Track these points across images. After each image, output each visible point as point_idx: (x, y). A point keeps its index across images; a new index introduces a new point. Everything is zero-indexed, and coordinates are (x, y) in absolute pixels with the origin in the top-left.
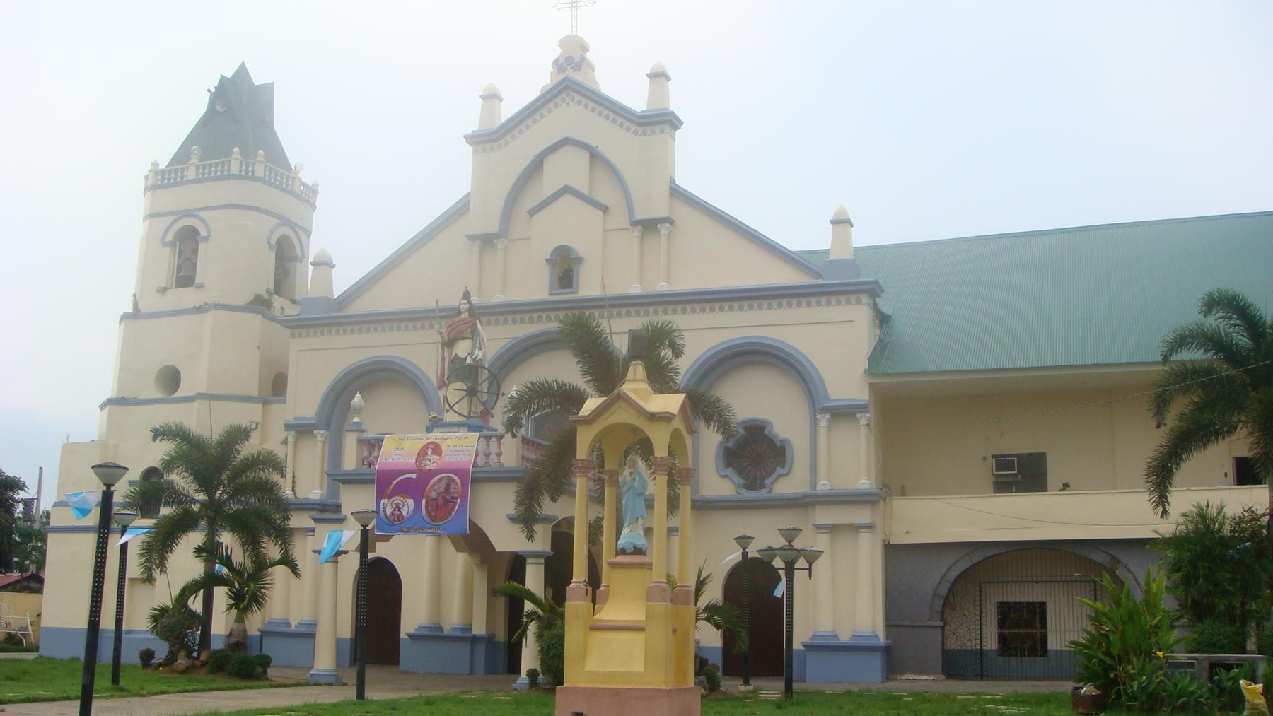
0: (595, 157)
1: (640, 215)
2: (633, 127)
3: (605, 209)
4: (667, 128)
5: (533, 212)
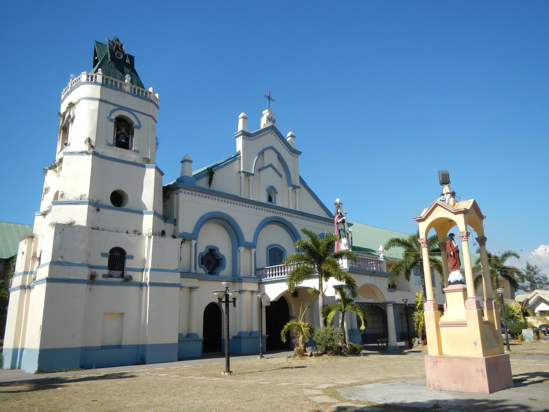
0: (280, 158)
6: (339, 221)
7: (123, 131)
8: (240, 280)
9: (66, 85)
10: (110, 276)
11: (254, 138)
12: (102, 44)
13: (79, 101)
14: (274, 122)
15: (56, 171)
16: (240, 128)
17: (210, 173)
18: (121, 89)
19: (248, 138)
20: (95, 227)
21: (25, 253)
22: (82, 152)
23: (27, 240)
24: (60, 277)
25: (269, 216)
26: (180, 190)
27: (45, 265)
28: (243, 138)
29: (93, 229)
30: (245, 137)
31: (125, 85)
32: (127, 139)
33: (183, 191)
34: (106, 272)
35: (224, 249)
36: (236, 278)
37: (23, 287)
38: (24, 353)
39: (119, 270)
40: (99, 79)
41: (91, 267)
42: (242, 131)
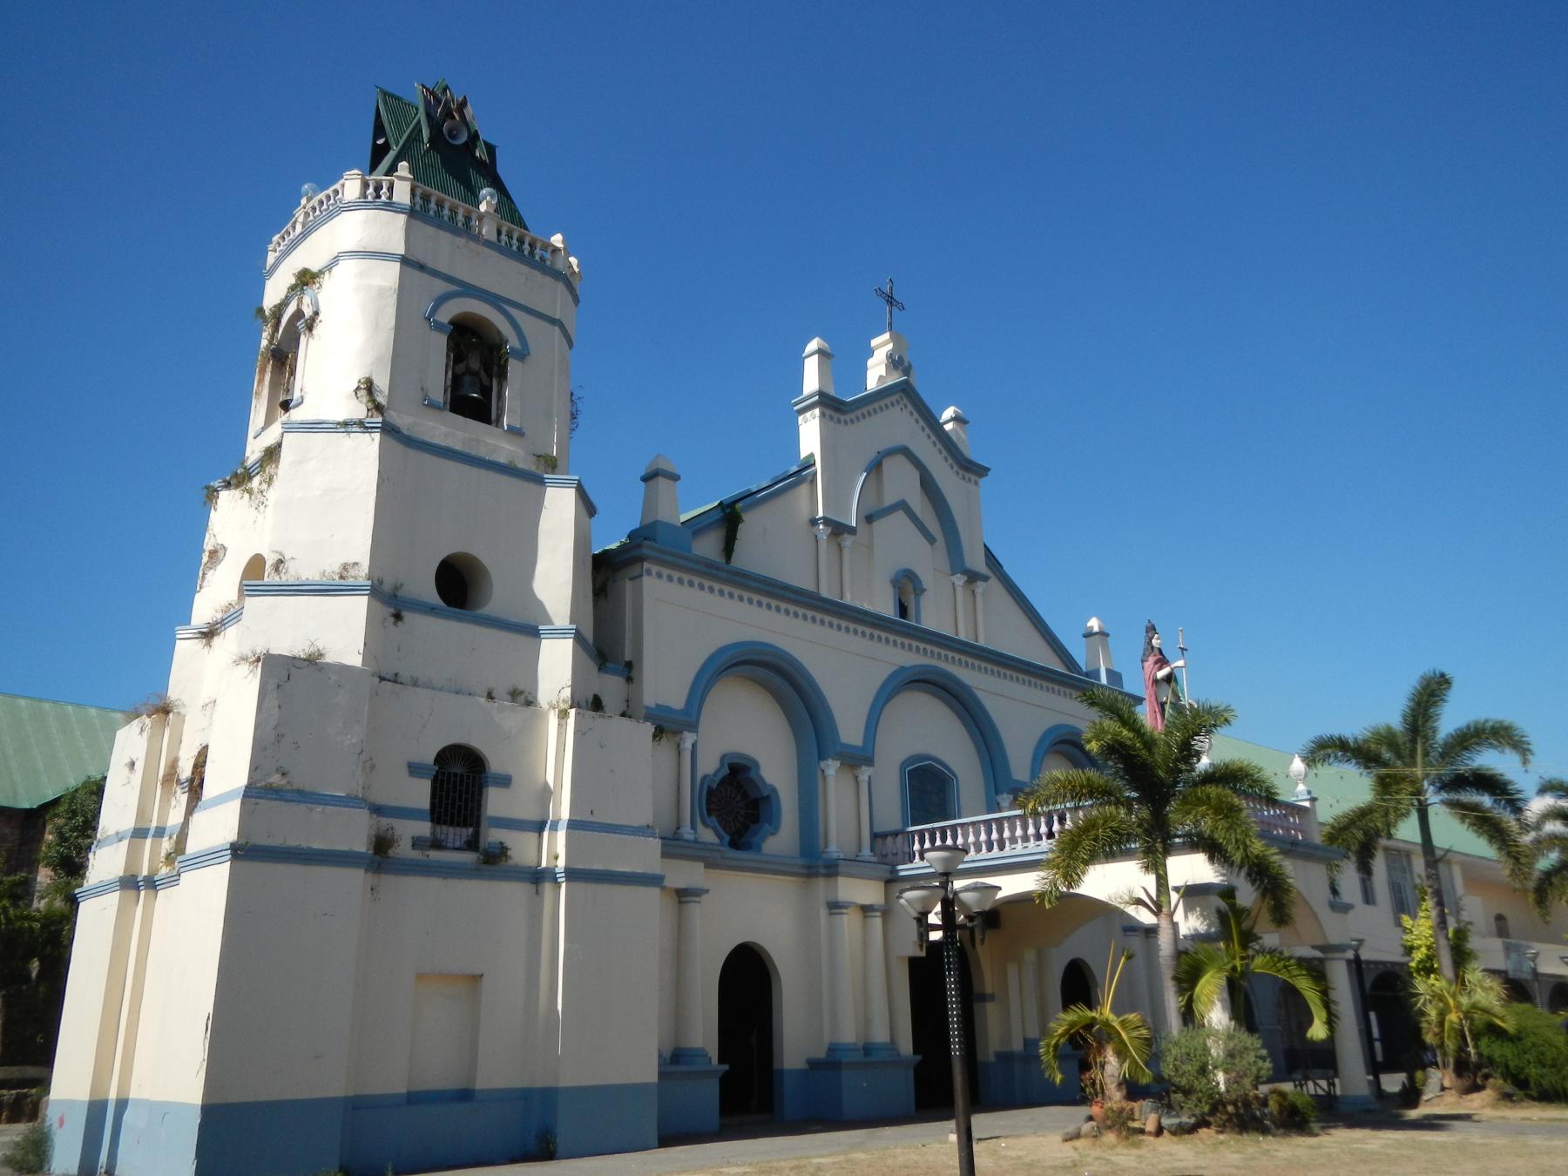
0: (928, 484)
6: (1161, 674)
7: (474, 363)
8: (831, 870)
9: (289, 215)
10: (437, 844)
11: (853, 416)
12: (398, 99)
13: (335, 261)
14: (907, 371)
15: (250, 492)
16: (811, 380)
17: (729, 517)
18: (466, 230)
19: (836, 415)
20: (388, 672)
21: (139, 766)
22: (346, 424)
23: (148, 721)
24: (276, 842)
25: (907, 664)
26: (646, 565)
27: (221, 799)
28: (823, 415)
29: (382, 679)
30: (828, 412)
31: (481, 217)
32: (486, 392)
33: (655, 569)
34: (424, 828)
35: (777, 769)
36: (815, 864)
37: (129, 883)
38: (127, 1117)
39: (465, 825)
40: (402, 192)
41: (377, 810)
42: (821, 393)
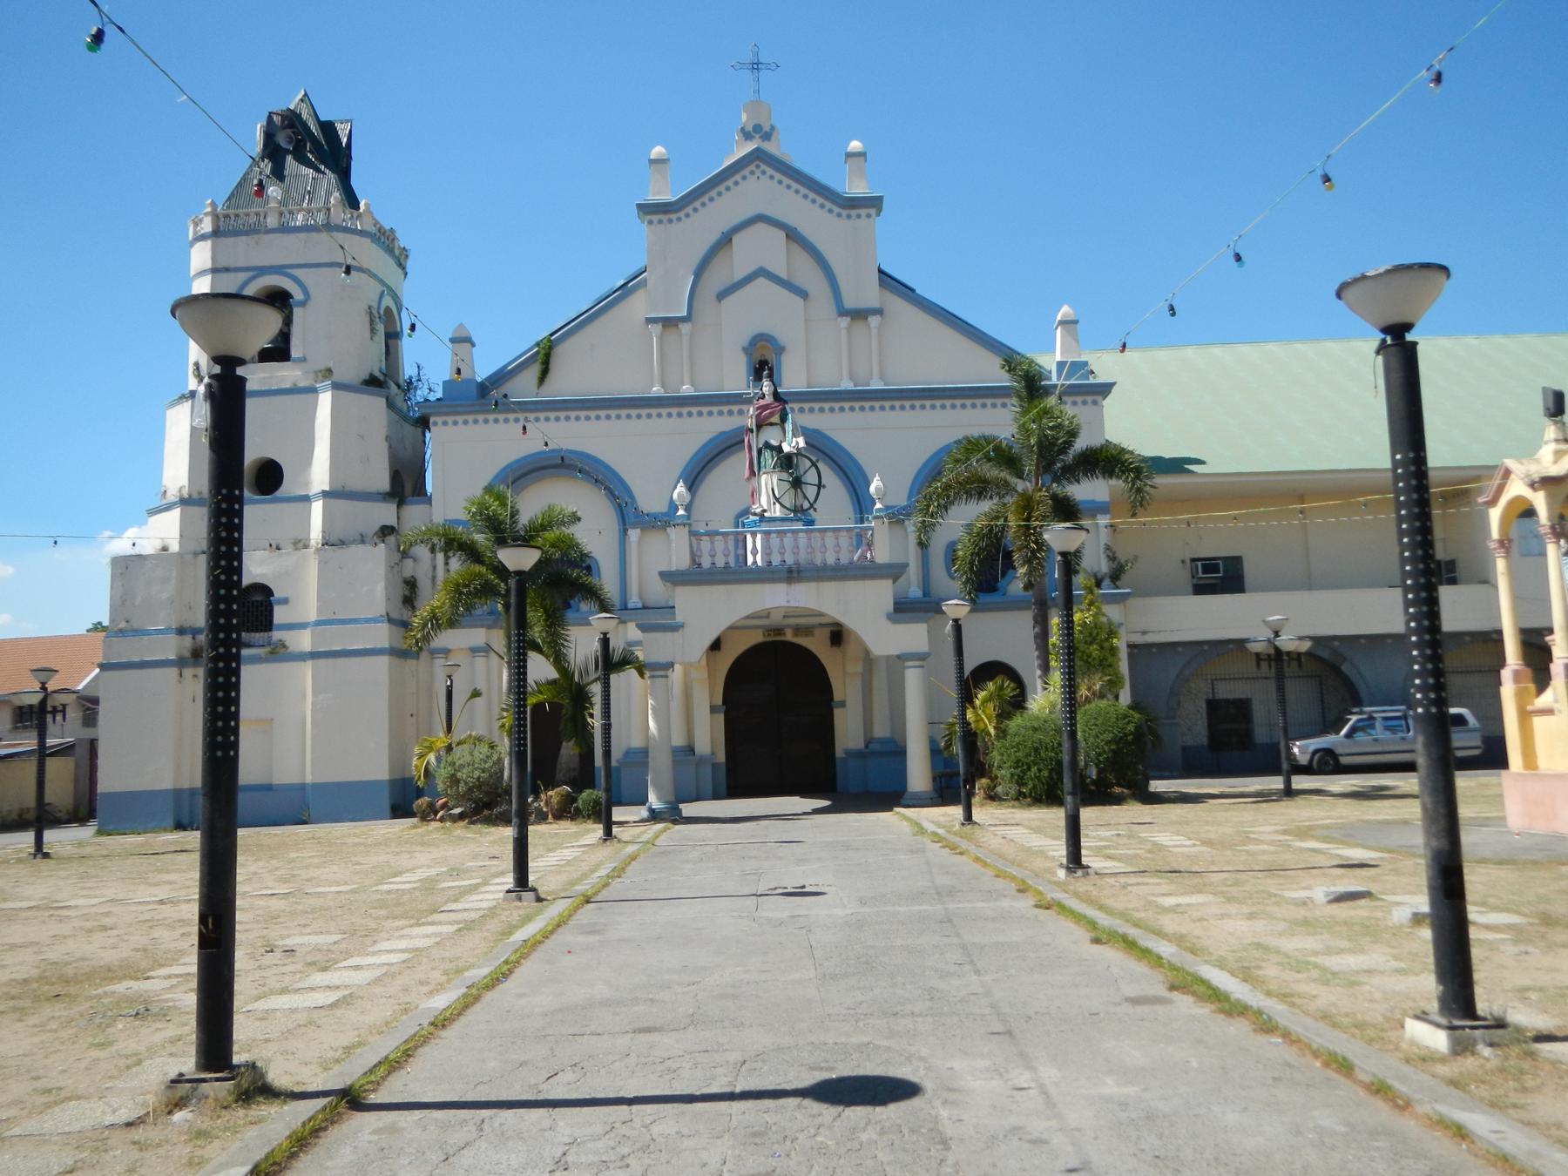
1: (850, 302)
2: (836, 210)
3: (803, 294)
4: (873, 211)
5: (722, 296)
25: (727, 429)
30: (655, 218)
33: (440, 420)
